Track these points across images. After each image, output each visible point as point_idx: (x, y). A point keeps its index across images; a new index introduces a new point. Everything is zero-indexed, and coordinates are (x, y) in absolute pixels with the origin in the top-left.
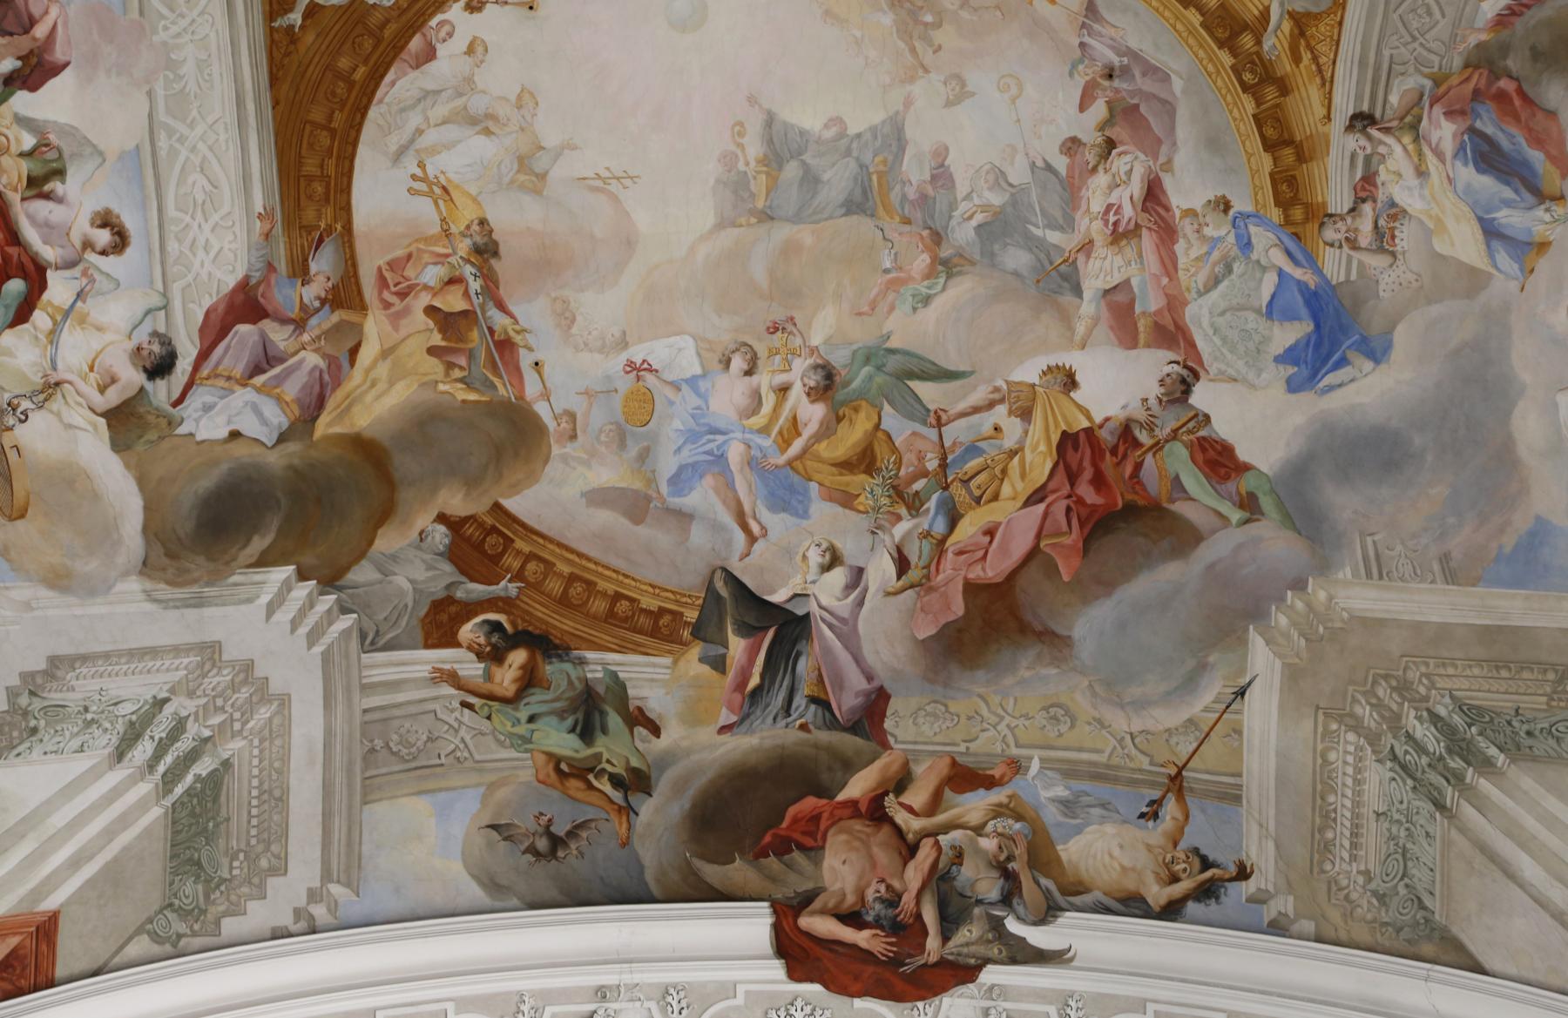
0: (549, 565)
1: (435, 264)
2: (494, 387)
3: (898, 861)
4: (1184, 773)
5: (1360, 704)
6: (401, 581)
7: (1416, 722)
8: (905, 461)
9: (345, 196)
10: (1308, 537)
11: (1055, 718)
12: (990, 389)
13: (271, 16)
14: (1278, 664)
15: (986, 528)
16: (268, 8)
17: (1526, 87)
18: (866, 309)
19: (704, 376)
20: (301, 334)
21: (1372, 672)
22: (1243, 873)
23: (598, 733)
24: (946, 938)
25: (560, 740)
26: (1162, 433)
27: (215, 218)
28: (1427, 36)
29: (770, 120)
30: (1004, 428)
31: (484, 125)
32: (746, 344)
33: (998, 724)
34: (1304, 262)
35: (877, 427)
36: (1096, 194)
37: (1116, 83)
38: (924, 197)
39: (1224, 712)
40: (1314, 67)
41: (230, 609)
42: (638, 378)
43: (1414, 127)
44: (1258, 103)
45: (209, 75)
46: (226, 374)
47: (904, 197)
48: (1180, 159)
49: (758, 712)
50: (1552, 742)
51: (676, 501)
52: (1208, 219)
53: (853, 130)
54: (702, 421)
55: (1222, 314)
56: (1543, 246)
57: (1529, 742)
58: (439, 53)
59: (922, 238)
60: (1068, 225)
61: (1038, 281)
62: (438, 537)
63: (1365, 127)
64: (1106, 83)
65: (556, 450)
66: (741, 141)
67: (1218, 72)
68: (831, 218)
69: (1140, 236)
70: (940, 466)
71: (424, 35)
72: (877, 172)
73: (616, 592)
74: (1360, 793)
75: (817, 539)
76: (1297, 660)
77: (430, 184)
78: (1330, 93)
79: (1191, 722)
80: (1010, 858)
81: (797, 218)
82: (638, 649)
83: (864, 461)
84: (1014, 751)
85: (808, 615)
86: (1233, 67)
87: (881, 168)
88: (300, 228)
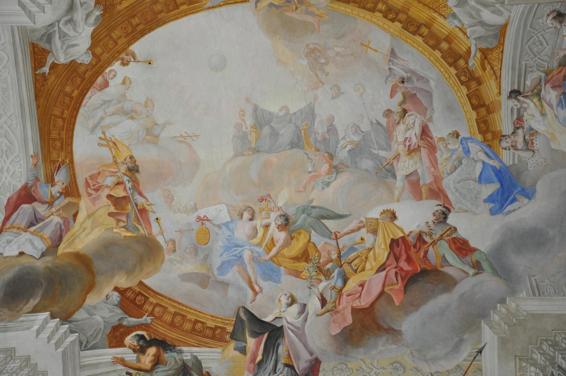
0: (165, 308)
1: (111, 176)
2: (139, 230)
5: (535, 353)
6: (98, 318)
7: (562, 360)
8: (322, 255)
9: (70, 147)
11: (396, 368)
12: (358, 222)
13: (35, 69)
14: (496, 337)
15: (360, 283)
16: (34, 65)
18: (302, 189)
19: (232, 221)
20: (51, 208)
21: (539, 338)
26: (436, 237)
27: (12, 157)
28: (541, 54)
29: (256, 109)
30: (365, 239)
31: (131, 115)
32: (250, 207)
33: (370, 372)
34: (494, 158)
35: (309, 241)
36: (400, 133)
37: (406, 85)
38: (325, 139)
39: (473, 361)
40: (492, 72)
41: (20, 333)
42: (203, 224)
43: (538, 94)
44: (468, 89)
45: (8, 95)
46: (18, 227)
47: (316, 140)
48: (436, 116)
49: (262, 372)
51: (221, 278)
52: (450, 141)
53: (292, 111)
54: (232, 242)
55: (459, 182)
58: (110, 84)
59: (325, 157)
60: (388, 148)
61: (377, 173)
62: (114, 298)
63: (516, 96)
64: (401, 85)
65: (167, 257)
66: (243, 118)
67: (450, 77)
68: (284, 150)
69: (420, 151)
70: (338, 257)
71: (103, 76)
72: (303, 129)
73: (196, 320)
75: (285, 292)
76: (504, 335)
77: (108, 141)
78: (500, 82)
79: (458, 366)
81: (270, 151)
82: (206, 345)
83: (304, 256)
85: (282, 327)
86: (456, 75)
87: (305, 127)
88: (50, 161)
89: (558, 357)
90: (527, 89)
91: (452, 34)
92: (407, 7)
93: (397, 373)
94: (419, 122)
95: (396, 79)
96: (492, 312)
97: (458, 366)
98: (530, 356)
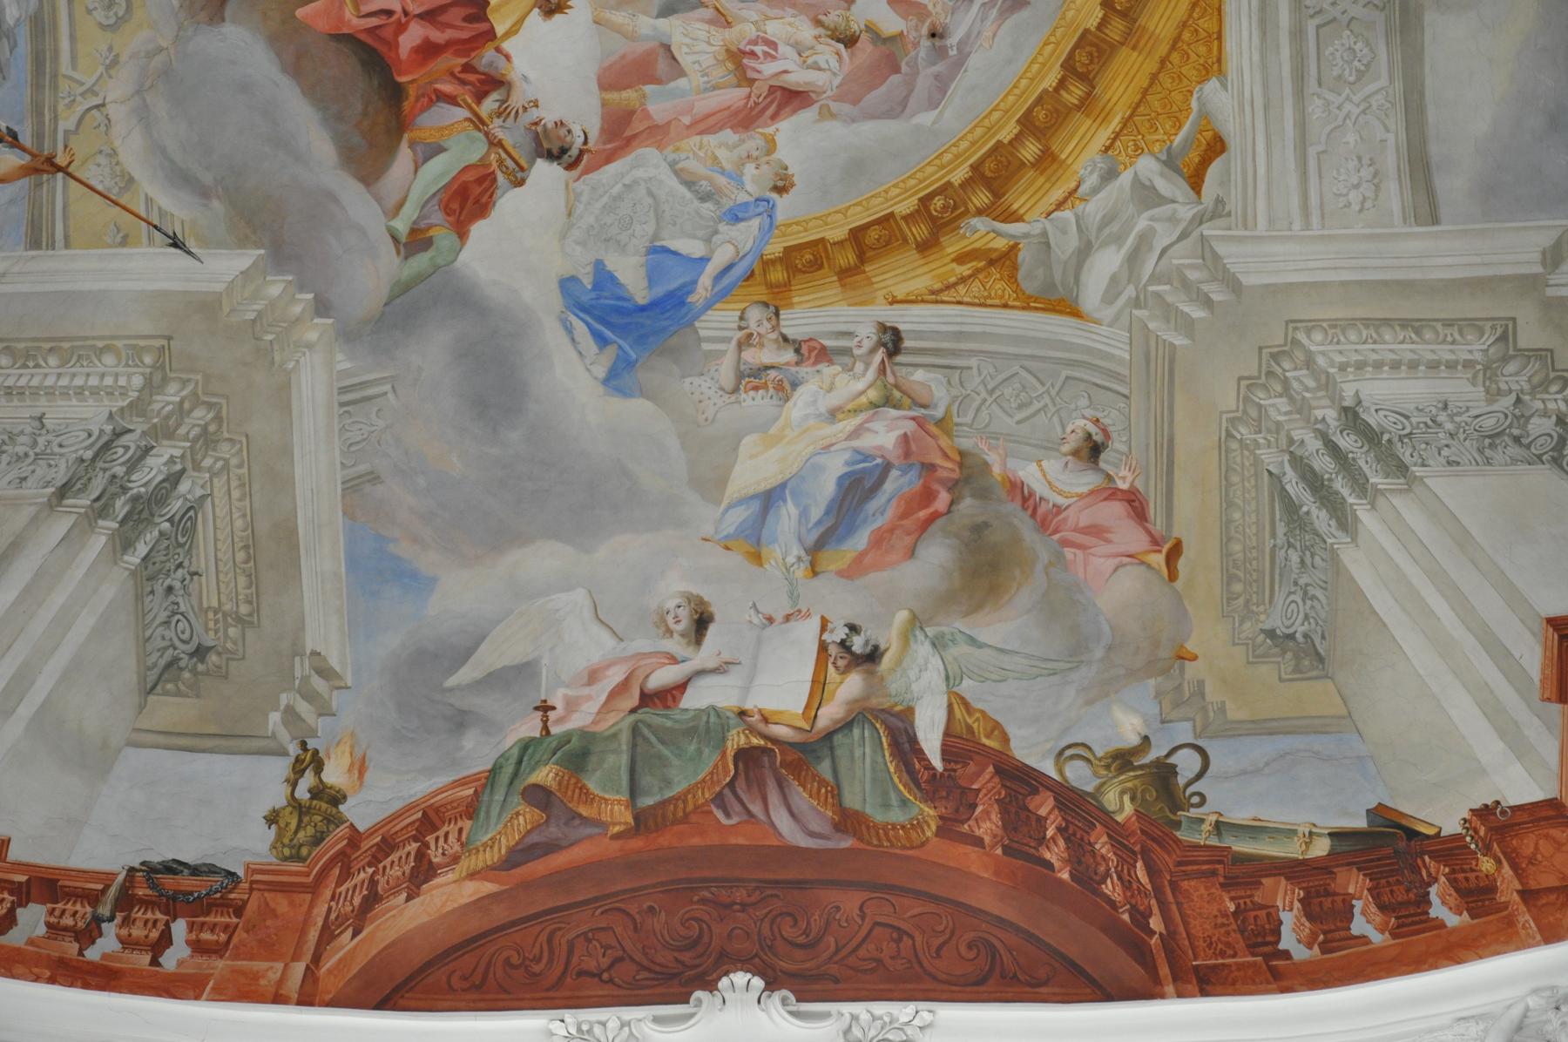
4: (60, 175)
7: (166, 457)
10: (383, 314)
14: (219, 287)
17: (940, 522)
21: (223, 401)
26: (496, 127)
28: (994, 406)
36: (788, 28)
37: (926, 43)
39: (149, 223)
40: (953, 280)
43: (888, 402)
44: (906, 218)
48: (836, 129)
50: (163, 616)
52: (764, 168)
55: (650, 193)
56: (757, 558)
57: (159, 588)
63: (884, 345)
64: (925, 31)
67: (943, 167)
69: (739, 86)
74: (65, 394)
76: (226, 310)
78: (923, 301)
86: (949, 183)
89: (175, 447)
90: (902, 371)
91: (1061, 171)
92: (1142, 43)
93: (96, 5)
94: (820, 83)
95: (943, 15)
96: (290, 278)
97: (131, 180)
98: (173, 375)
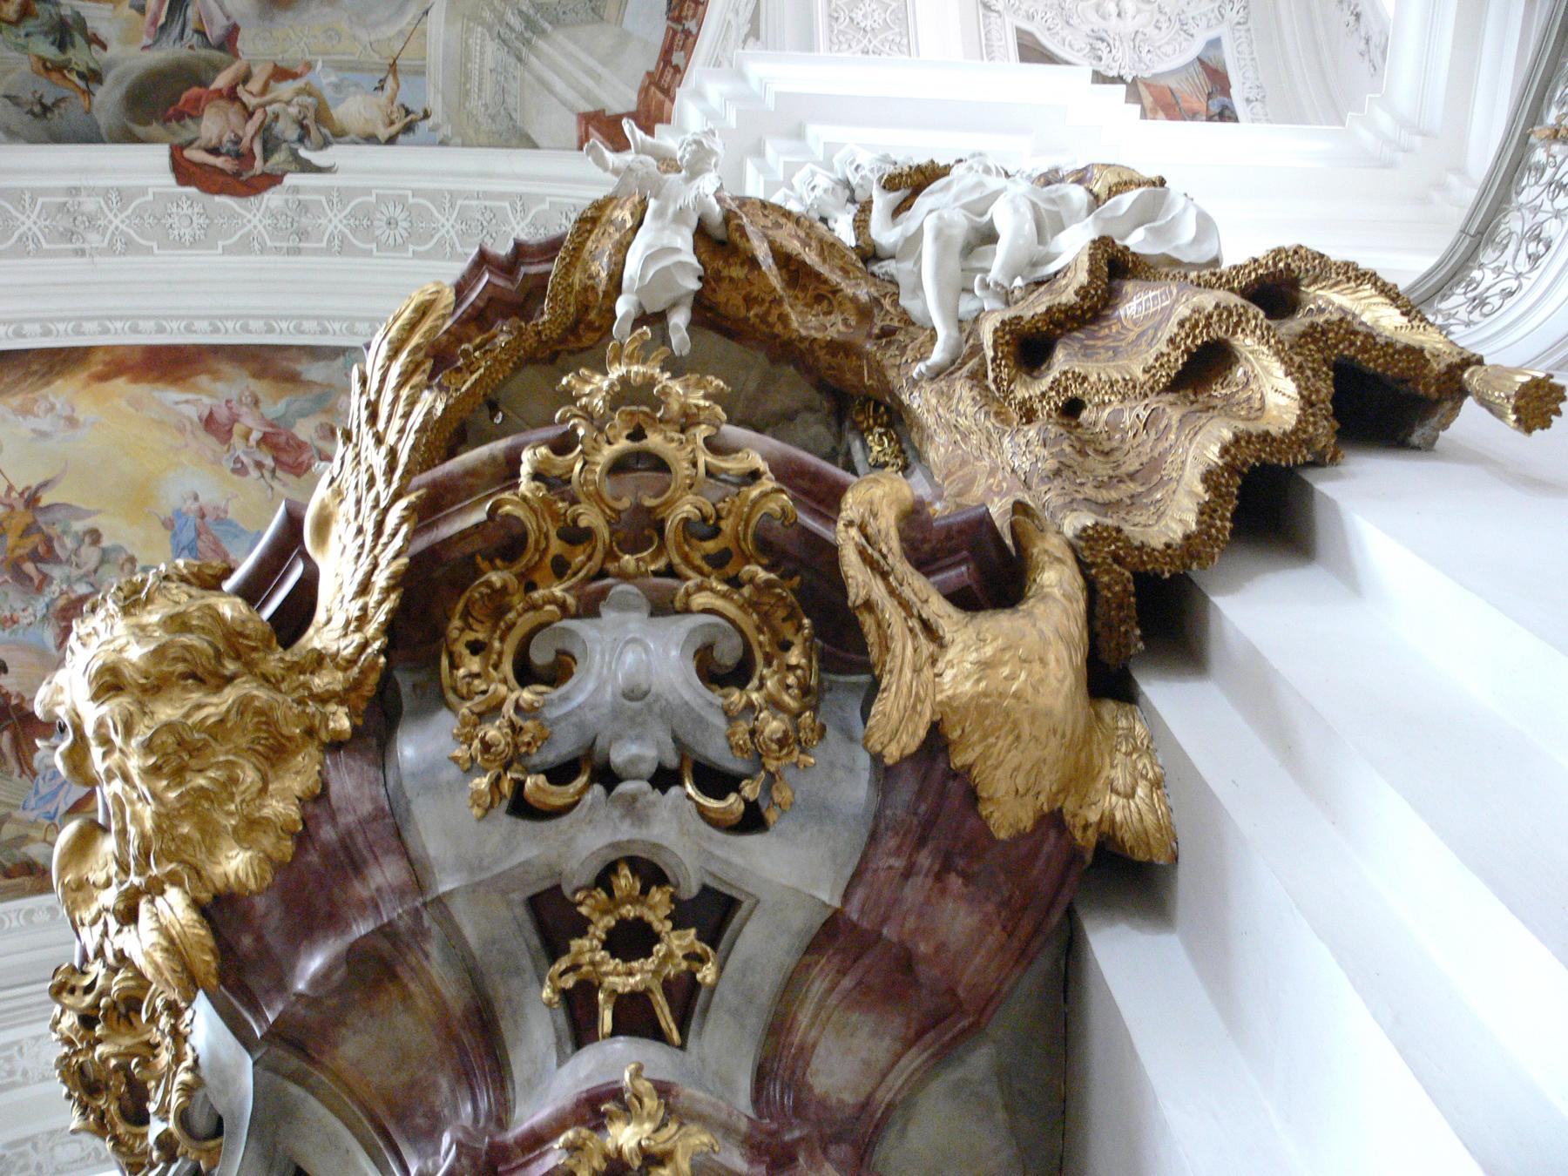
3: (242, 122)
22: (426, 115)
23: (69, 46)
24: (266, 160)
25: (49, 51)
79: (401, 32)
80: (305, 118)
84: (308, 57)
